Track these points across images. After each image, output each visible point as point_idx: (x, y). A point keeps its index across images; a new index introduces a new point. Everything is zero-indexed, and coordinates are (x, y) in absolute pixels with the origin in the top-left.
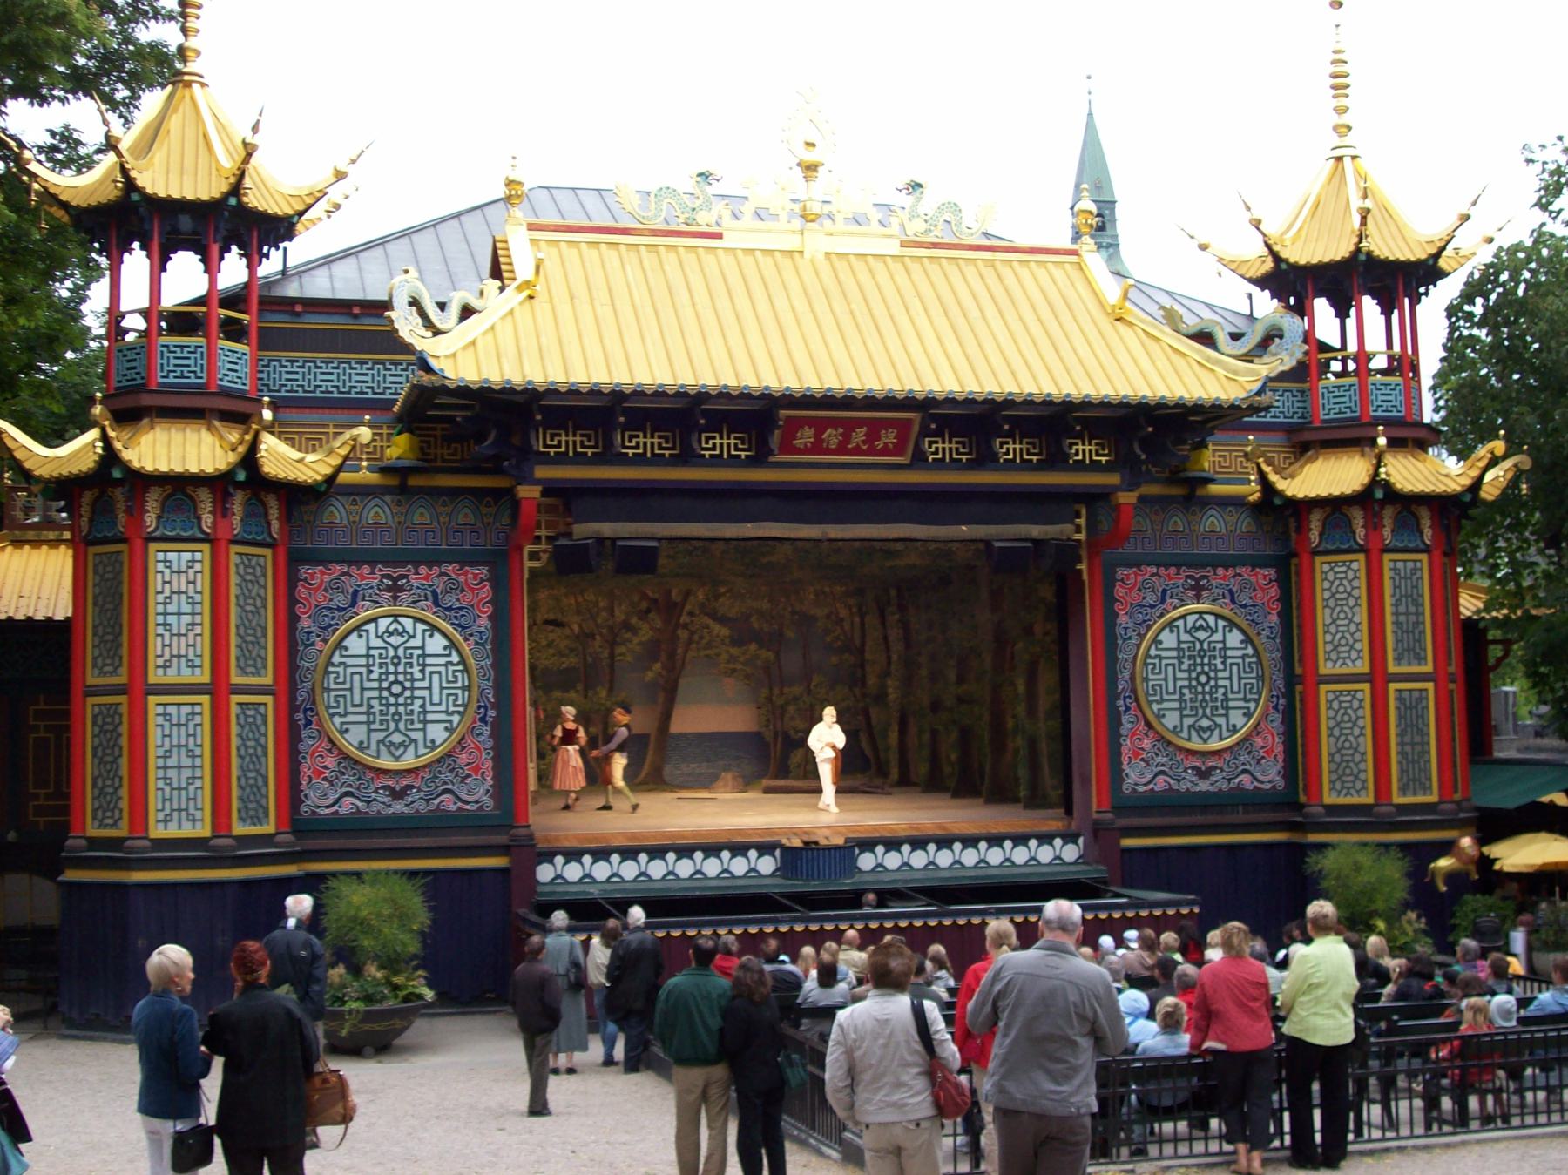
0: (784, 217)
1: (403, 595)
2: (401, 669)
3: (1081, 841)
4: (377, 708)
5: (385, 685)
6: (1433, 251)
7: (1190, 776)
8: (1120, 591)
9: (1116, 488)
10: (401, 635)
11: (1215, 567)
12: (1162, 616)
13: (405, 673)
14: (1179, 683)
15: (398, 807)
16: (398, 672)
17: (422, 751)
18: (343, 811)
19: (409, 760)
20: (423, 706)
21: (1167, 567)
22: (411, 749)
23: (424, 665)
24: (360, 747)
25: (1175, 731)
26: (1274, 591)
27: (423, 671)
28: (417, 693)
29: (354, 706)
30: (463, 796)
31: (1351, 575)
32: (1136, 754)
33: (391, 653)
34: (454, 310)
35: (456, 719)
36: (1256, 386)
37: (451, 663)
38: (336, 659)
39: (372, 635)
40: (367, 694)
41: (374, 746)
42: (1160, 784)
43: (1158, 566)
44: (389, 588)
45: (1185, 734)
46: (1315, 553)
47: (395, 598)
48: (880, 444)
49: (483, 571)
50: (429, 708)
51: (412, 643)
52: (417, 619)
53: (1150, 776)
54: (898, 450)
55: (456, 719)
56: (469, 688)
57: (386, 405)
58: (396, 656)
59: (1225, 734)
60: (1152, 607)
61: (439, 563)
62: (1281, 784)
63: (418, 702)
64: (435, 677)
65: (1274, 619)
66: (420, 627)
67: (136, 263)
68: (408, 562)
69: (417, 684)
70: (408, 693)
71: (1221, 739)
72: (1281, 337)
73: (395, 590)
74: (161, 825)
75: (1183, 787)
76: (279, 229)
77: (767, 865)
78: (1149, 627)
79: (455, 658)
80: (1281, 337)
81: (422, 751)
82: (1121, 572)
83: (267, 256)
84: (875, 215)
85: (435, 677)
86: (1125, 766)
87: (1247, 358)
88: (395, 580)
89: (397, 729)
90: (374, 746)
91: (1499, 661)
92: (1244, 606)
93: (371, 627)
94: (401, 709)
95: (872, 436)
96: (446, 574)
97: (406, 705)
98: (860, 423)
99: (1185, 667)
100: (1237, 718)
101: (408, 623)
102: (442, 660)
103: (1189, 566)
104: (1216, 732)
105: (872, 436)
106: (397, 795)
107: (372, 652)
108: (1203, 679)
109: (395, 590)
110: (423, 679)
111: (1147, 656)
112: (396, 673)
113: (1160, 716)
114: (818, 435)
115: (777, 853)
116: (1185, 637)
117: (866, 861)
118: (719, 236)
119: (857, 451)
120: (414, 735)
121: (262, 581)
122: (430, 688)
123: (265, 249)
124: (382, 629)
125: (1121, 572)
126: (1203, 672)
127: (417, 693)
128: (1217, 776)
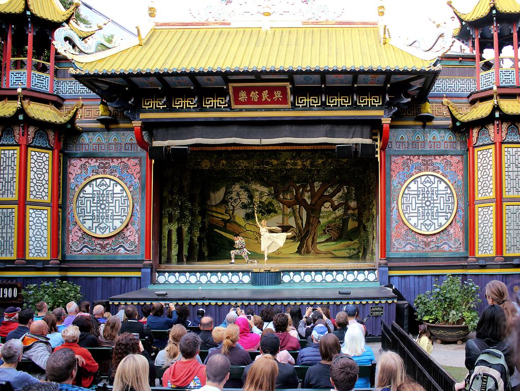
8: (393, 166)
12: (411, 176)
16: (101, 199)
17: (112, 230)
22: (108, 230)
26: (461, 166)
37: (123, 196)
38: (81, 195)
42: (408, 248)
44: (102, 168)
45: (419, 227)
49: (137, 161)
53: (404, 245)
55: (124, 218)
59: (437, 227)
61: (121, 158)
62: (462, 250)
63: (111, 211)
64: (117, 202)
66: (112, 182)
71: (435, 229)
73: (105, 167)
77: (247, 279)
81: (112, 230)
82: (393, 158)
93: (94, 183)
96: (123, 162)
99: (420, 198)
100: (442, 220)
110: (112, 203)
111: (404, 193)
116: (420, 186)
117: (286, 278)
122: (115, 206)
124: (98, 183)
125: (393, 158)
126: (428, 201)
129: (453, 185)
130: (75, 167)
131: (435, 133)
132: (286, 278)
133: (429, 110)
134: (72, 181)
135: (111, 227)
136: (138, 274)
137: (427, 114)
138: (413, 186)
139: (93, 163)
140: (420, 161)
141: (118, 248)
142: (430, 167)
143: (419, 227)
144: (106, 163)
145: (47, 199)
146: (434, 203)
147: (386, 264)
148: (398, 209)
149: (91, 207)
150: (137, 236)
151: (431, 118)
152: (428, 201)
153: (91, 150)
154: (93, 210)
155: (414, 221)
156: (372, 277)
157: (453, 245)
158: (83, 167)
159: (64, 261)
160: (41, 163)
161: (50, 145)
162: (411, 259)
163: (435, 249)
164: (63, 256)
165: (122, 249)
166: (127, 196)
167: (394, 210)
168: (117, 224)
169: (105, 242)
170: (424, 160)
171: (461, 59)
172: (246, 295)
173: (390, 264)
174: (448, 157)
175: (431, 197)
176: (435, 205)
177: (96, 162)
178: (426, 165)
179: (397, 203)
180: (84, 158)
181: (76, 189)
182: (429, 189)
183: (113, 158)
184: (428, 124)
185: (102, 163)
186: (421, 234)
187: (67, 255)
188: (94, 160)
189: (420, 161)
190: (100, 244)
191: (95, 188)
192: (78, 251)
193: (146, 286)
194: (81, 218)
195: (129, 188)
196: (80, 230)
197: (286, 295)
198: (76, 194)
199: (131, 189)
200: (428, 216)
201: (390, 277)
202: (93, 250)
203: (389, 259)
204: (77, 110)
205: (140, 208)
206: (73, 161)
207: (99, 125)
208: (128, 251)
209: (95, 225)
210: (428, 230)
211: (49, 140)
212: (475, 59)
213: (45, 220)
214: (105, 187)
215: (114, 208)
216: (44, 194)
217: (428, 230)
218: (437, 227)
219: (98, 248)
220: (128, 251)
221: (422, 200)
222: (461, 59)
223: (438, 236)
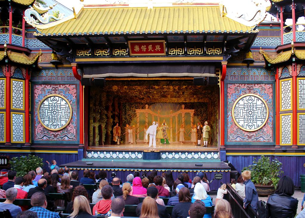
5: (52, 112)
8: (229, 90)
10: (56, 100)
11: (255, 84)
12: (240, 96)
14: (244, 114)
15: (55, 139)
16: (54, 109)
17: (60, 127)
19: (57, 129)
20: (60, 116)
21: (242, 84)
22: (58, 126)
23: (61, 107)
25: (242, 126)
26: (271, 90)
29: (46, 116)
30: (69, 137)
38: (42, 106)
42: (238, 139)
43: (239, 84)
44: (54, 90)
45: (245, 127)
46: (279, 79)
47: (55, 92)
49: (74, 86)
50: (62, 117)
52: (59, 97)
55: (67, 120)
58: (55, 106)
59: (256, 127)
61: (65, 84)
62: (271, 141)
64: (63, 110)
65: (271, 97)
68: (58, 84)
71: (255, 129)
73: (55, 90)
77: (140, 156)
78: (236, 99)
81: (60, 127)
82: (229, 86)
86: (229, 135)
88: (55, 88)
93: (49, 99)
96: (66, 87)
100: (259, 123)
103: (248, 84)
106: (55, 136)
107: (49, 105)
108: (55, 113)
109: (55, 90)
113: (238, 123)
117: (164, 156)
118: (128, 5)
122: (62, 113)
124: (52, 99)
125: (229, 86)
129: (266, 102)
130: (39, 90)
131: (255, 70)
132: (164, 156)
133: (251, 57)
134: (37, 98)
135: (60, 125)
136: (76, 152)
137: (250, 59)
138: (241, 102)
139: (49, 87)
140: (245, 87)
141: (64, 137)
142: (252, 91)
143: (245, 127)
144: (56, 88)
145: (22, 108)
146: (254, 113)
147: (224, 149)
148: (232, 116)
149: (48, 113)
150: (75, 130)
151: (252, 62)
152: (250, 111)
153: (47, 80)
154: (49, 115)
155: (241, 123)
156: (216, 156)
157: (267, 138)
158: (43, 90)
159: (33, 144)
160: (18, 87)
161: (23, 77)
162: (240, 146)
163: (255, 140)
164: (33, 141)
165: (66, 137)
166: (69, 107)
167: (230, 116)
168: (63, 123)
169: (57, 134)
170: (248, 87)
171: (271, 25)
172: (140, 165)
173: (227, 149)
174: (263, 85)
175: (252, 109)
176: (255, 114)
177: (51, 87)
178: (250, 90)
179: (231, 113)
180: (43, 84)
181: (39, 103)
182: (251, 104)
183: (60, 84)
184: (251, 65)
185: (54, 88)
186: (246, 131)
187: (35, 140)
188: (49, 86)
189: (245, 87)
190: (53, 135)
191: (50, 102)
192: (41, 138)
193: (81, 159)
194: (42, 119)
195: (70, 102)
196: (42, 126)
197: (164, 165)
198: (39, 105)
199: (71, 103)
200: (250, 120)
201: (227, 156)
202: (49, 138)
203: (226, 146)
204: (39, 56)
205: (77, 114)
206: (37, 86)
207: (51, 65)
208: (70, 139)
210: (250, 129)
211: (23, 74)
212: (280, 25)
213: (22, 120)
214: (56, 102)
215: (61, 114)
216: (20, 105)
217: (250, 129)
218: (256, 127)
219: (53, 136)
220: (70, 139)
221: (247, 111)
222: (271, 25)
223: (256, 132)
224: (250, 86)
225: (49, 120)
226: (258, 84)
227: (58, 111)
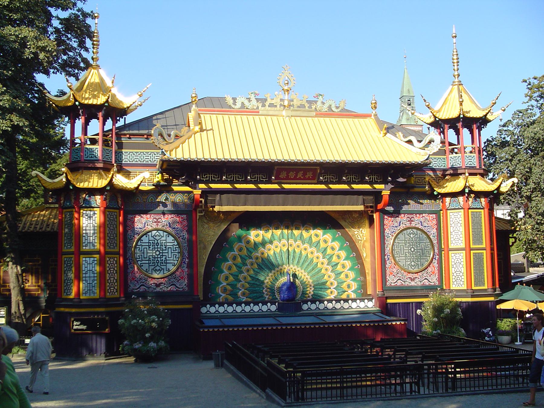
0: (278, 106)
1: (160, 224)
2: (159, 247)
3: (373, 300)
4: (152, 259)
6: (485, 114)
7: (409, 280)
9: (383, 189)
11: (416, 214)
13: (160, 248)
14: (405, 251)
17: (165, 272)
18: (141, 290)
20: (166, 258)
24: (146, 271)
26: (435, 222)
27: (166, 247)
28: (164, 254)
31: (459, 216)
32: (391, 273)
33: (156, 242)
34: (173, 136)
35: (176, 262)
36: (426, 157)
39: (150, 236)
40: (149, 254)
41: (150, 270)
42: (399, 283)
48: (307, 176)
51: (163, 239)
52: (164, 231)
53: (395, 281)
54: (313, 178)
56: (180, 253)
57: (155, 165)
60: (396, 227)
62: (437, 283)
64: (170, 249)
66: (165, 234)
67: (79, 123)
69: (164, 251)
70: (161, 254)
72: (433, 141)
74: (84, 295)
75: (407, 283)
76: (123, 112)
79: (176, 243)
80: (433, 141)
81: (165, 272)
83: (119, 120)
84: (307, 105)
85: (170, 249)
86: (388, 277)
87: (423, 149)
88: (157, 219)
89: (158, 265)
90: (150, 270)
91: (513, 243)
92: (425, 227)
94: (159, 259)
95: (305, 174)
97: (160, 258)
98: (301, 170)
101: (161, 232)
102: (172, 244)
103: (408, 214)
104: (417, 267)
105: (305, 174)
112: (158, 248)
114: (287, 174)
115: (277, 304)
116: (407, 236)
117: (305, 307)
119: (300, 179)
120: (163, 267)
121: (116, 220)
123: (118, 118)
127: (164, 254)
128: (417, 280)
135: (165, 270)
191: (151, 238)
209: (151, 267)
224: (410, 216)
225: (149, 263)
226: (420, 214)
227: (163, 250)
